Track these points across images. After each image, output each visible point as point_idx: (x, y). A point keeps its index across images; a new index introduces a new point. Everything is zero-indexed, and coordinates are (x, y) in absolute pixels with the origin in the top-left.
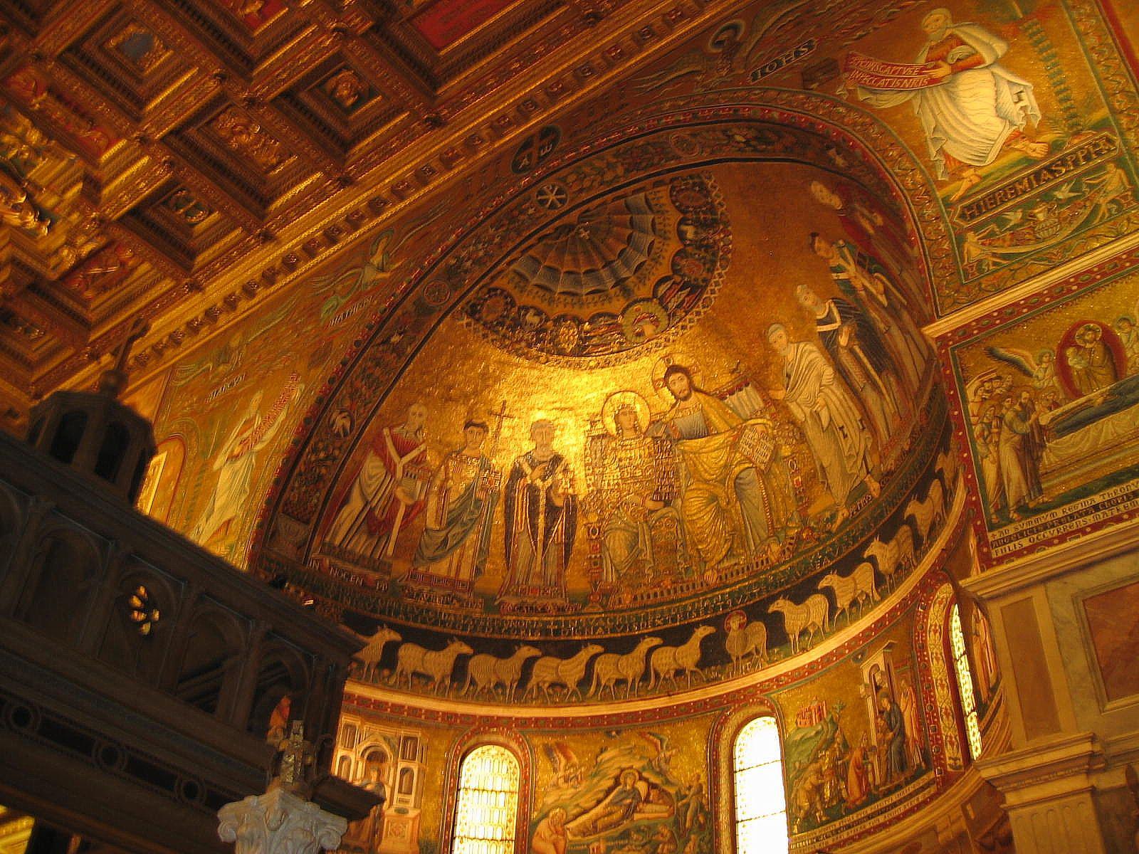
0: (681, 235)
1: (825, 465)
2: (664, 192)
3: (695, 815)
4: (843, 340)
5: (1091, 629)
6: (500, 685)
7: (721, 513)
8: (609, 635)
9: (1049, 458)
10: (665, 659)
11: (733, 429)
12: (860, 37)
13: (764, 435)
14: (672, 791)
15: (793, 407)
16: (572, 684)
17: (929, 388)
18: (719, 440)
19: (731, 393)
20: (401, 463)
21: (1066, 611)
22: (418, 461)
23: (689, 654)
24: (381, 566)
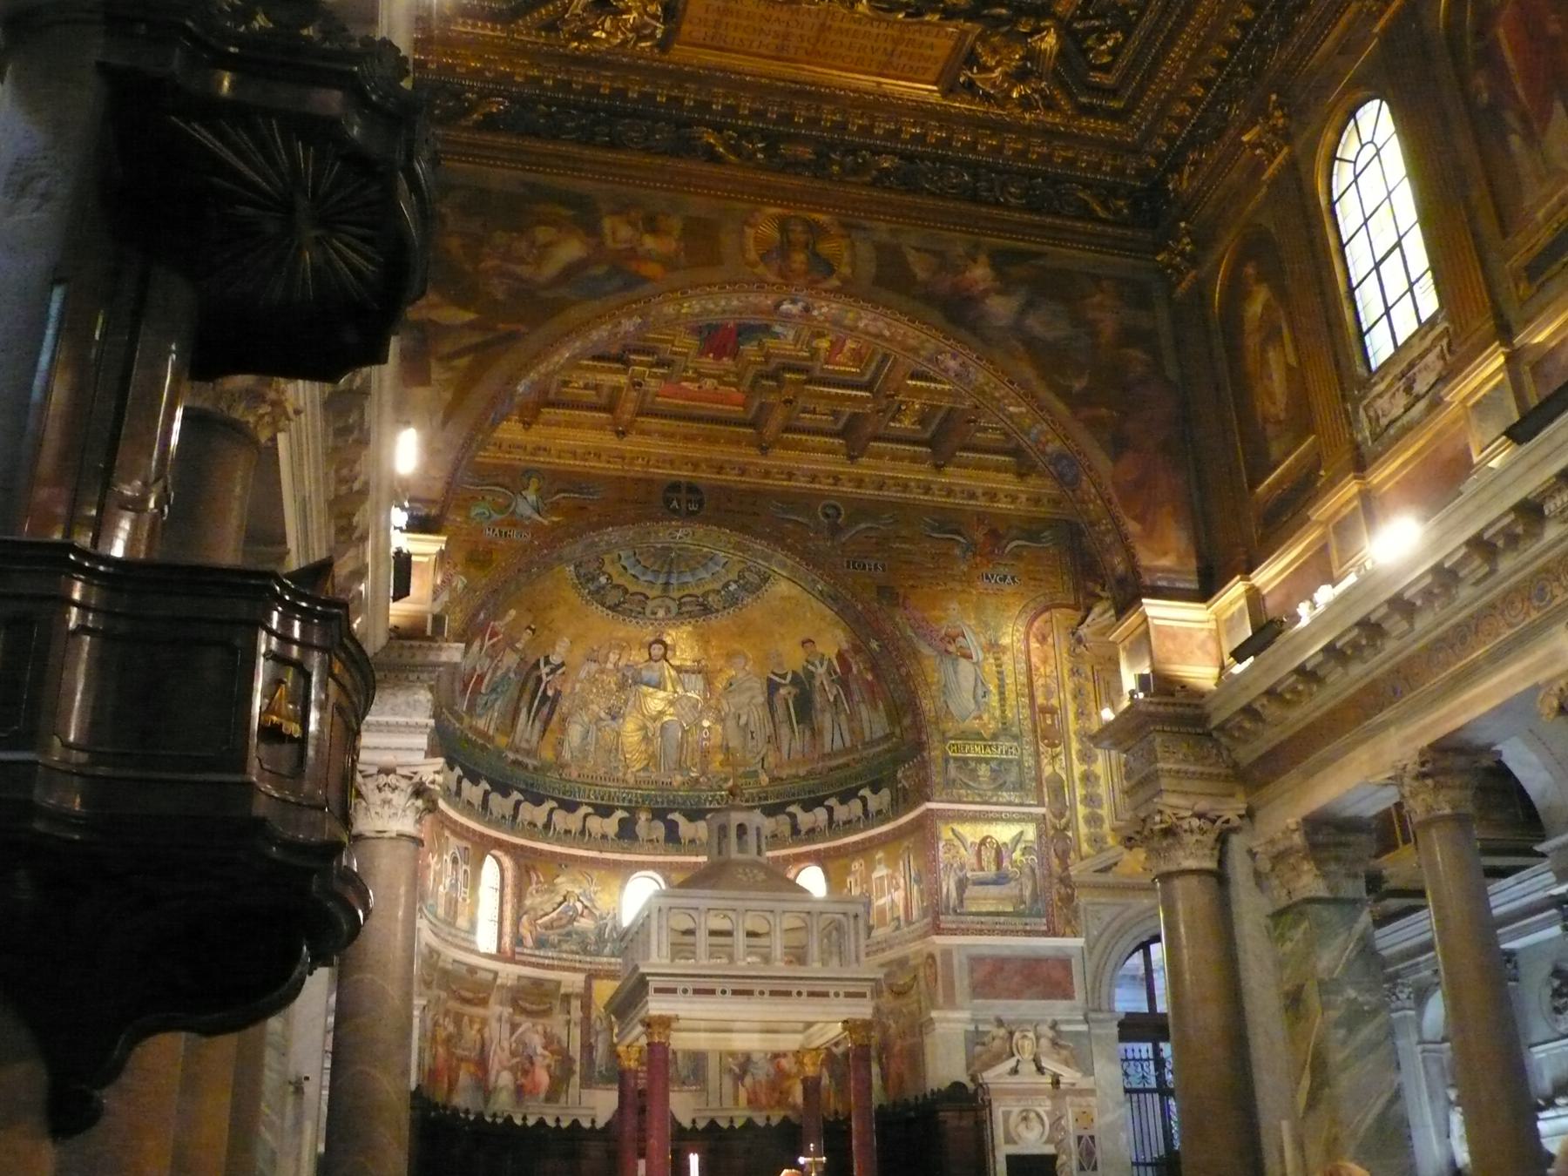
0: (726, 585)
1: (731, 745)
2: (743, 566)
3: (611, 931)
4: (783, 691)
5: (972, 971)
6: (503, 817)
7: (646, 739)
8: (561, 796)
9: (967, 894)
10: (595, 824)
11: (675, 692)
12: (912, 586)
13: (695, 706)
14: (597, 913)
15: (724, 702)
16: (540, 824)
17: (841, 761)
18: (661, 694)
19: (686, 672)
20: (487, 643)
21: (965, 961)
22: (493, 645)
23: (611, 825)
24: (460, 719)
